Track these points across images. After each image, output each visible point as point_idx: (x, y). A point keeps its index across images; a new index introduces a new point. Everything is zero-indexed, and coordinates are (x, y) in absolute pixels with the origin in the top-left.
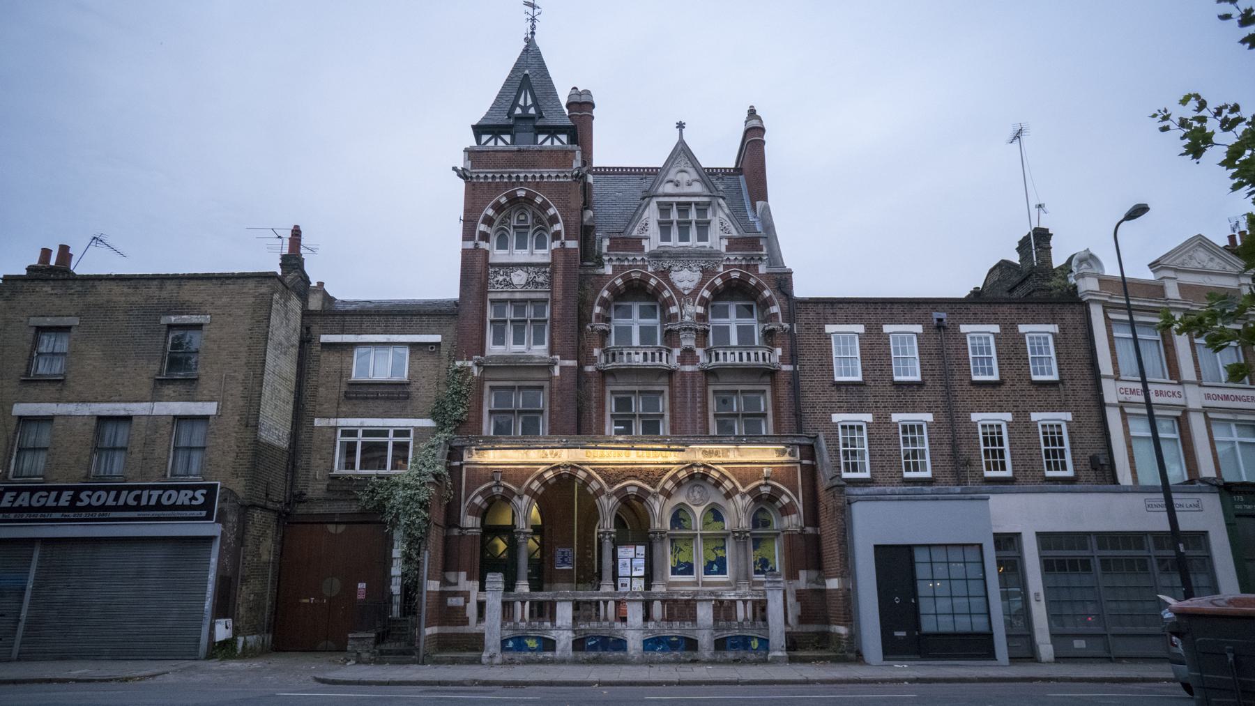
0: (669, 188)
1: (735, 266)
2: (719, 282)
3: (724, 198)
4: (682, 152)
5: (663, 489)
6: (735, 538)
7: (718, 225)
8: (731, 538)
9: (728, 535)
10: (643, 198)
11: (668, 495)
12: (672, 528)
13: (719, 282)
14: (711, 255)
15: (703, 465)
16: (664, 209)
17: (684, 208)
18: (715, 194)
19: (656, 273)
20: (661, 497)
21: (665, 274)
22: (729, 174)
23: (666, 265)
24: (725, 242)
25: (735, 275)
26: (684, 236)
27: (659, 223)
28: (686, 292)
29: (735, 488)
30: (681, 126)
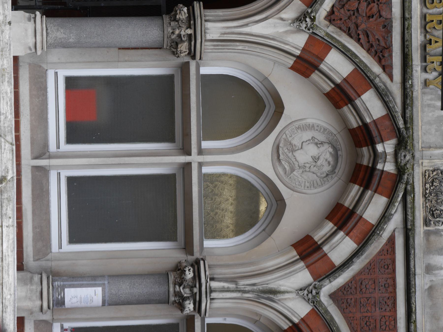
5: (328, 45)
6: (179, 269)
8: (180, 256)
9: (188, 247)
11: (306, 64)
12: (208, 81)
15: (401, 170)
20: (298, 41)
29: (334, 271)
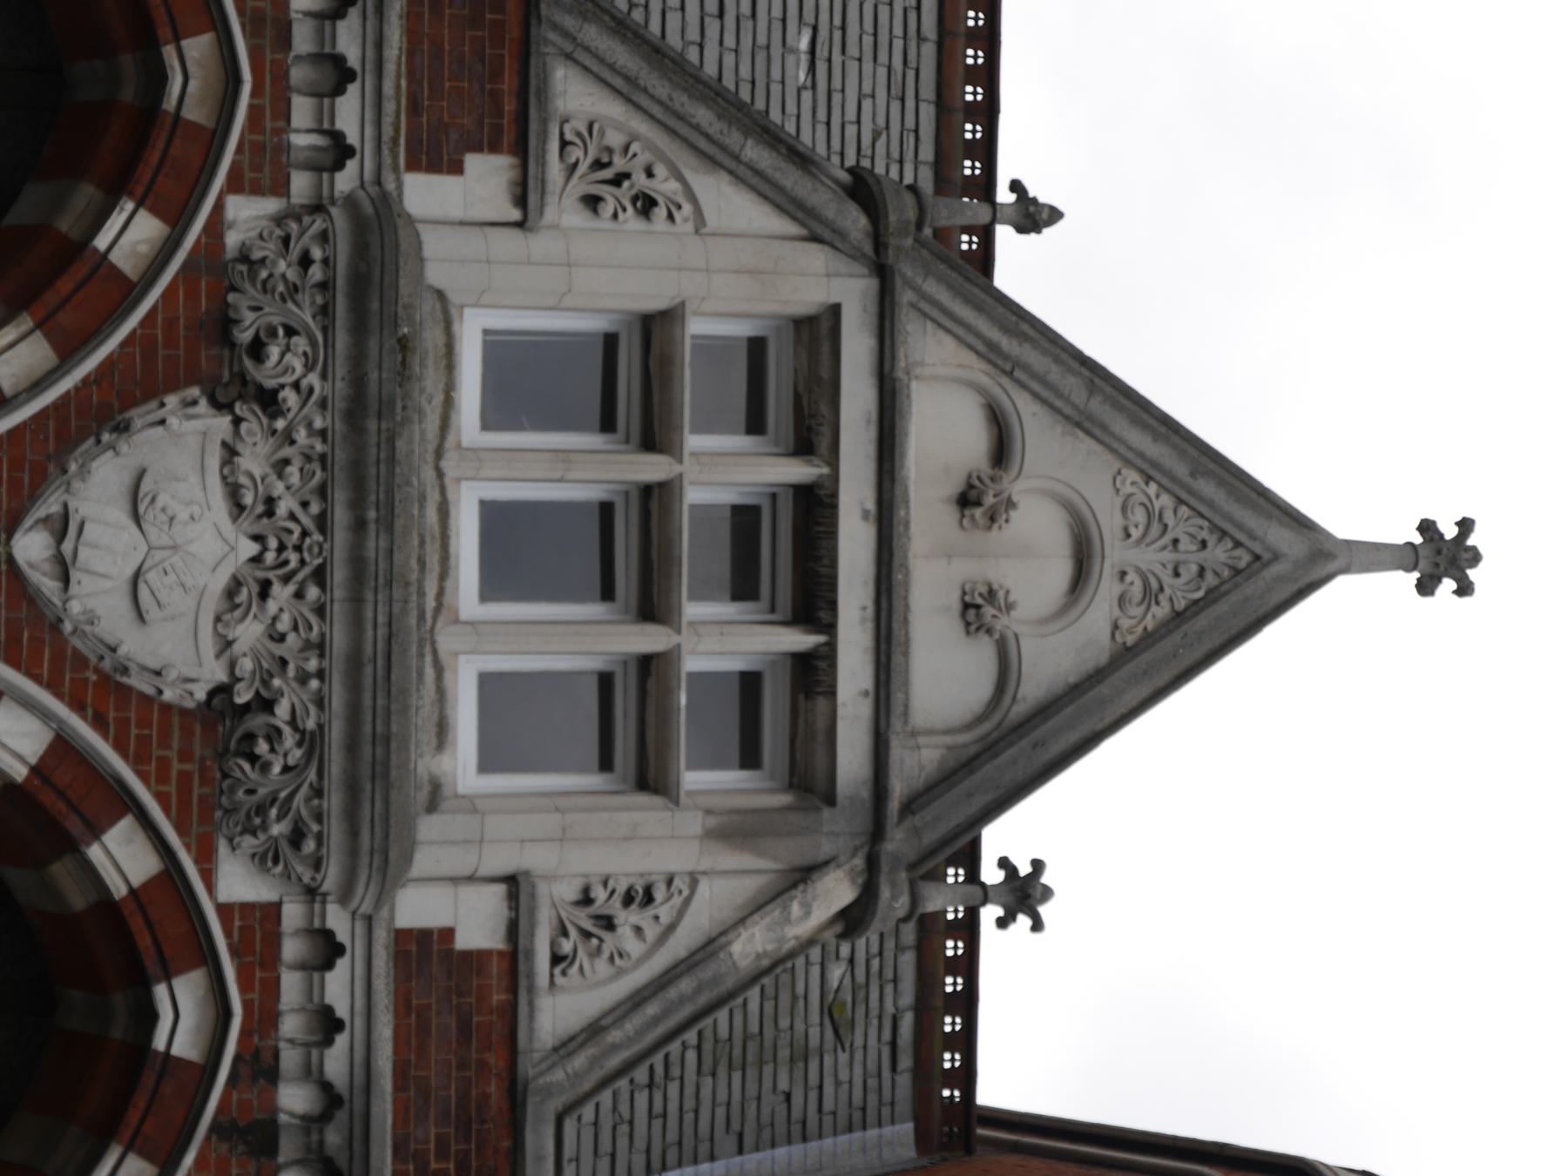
0: (944, 431)
1: (264, 1016)
2: (122, 857)
3: (852, 920)
4: (1223, 560)
7: (629, 864)
10: (862, 189)
13: (122, 857)
14: (370, 795)
16: (787, 387)
17: (786, 554)
18: (897, 841)
19: (216, 271)
21: (207, 352)
22: (927, 1041)
23: (283, 365)
24: (477, 924)
25: (180, 1018)
26: (520, 548)
27: (656, 328)
28: (31, 547)
30: (1442, 558)
